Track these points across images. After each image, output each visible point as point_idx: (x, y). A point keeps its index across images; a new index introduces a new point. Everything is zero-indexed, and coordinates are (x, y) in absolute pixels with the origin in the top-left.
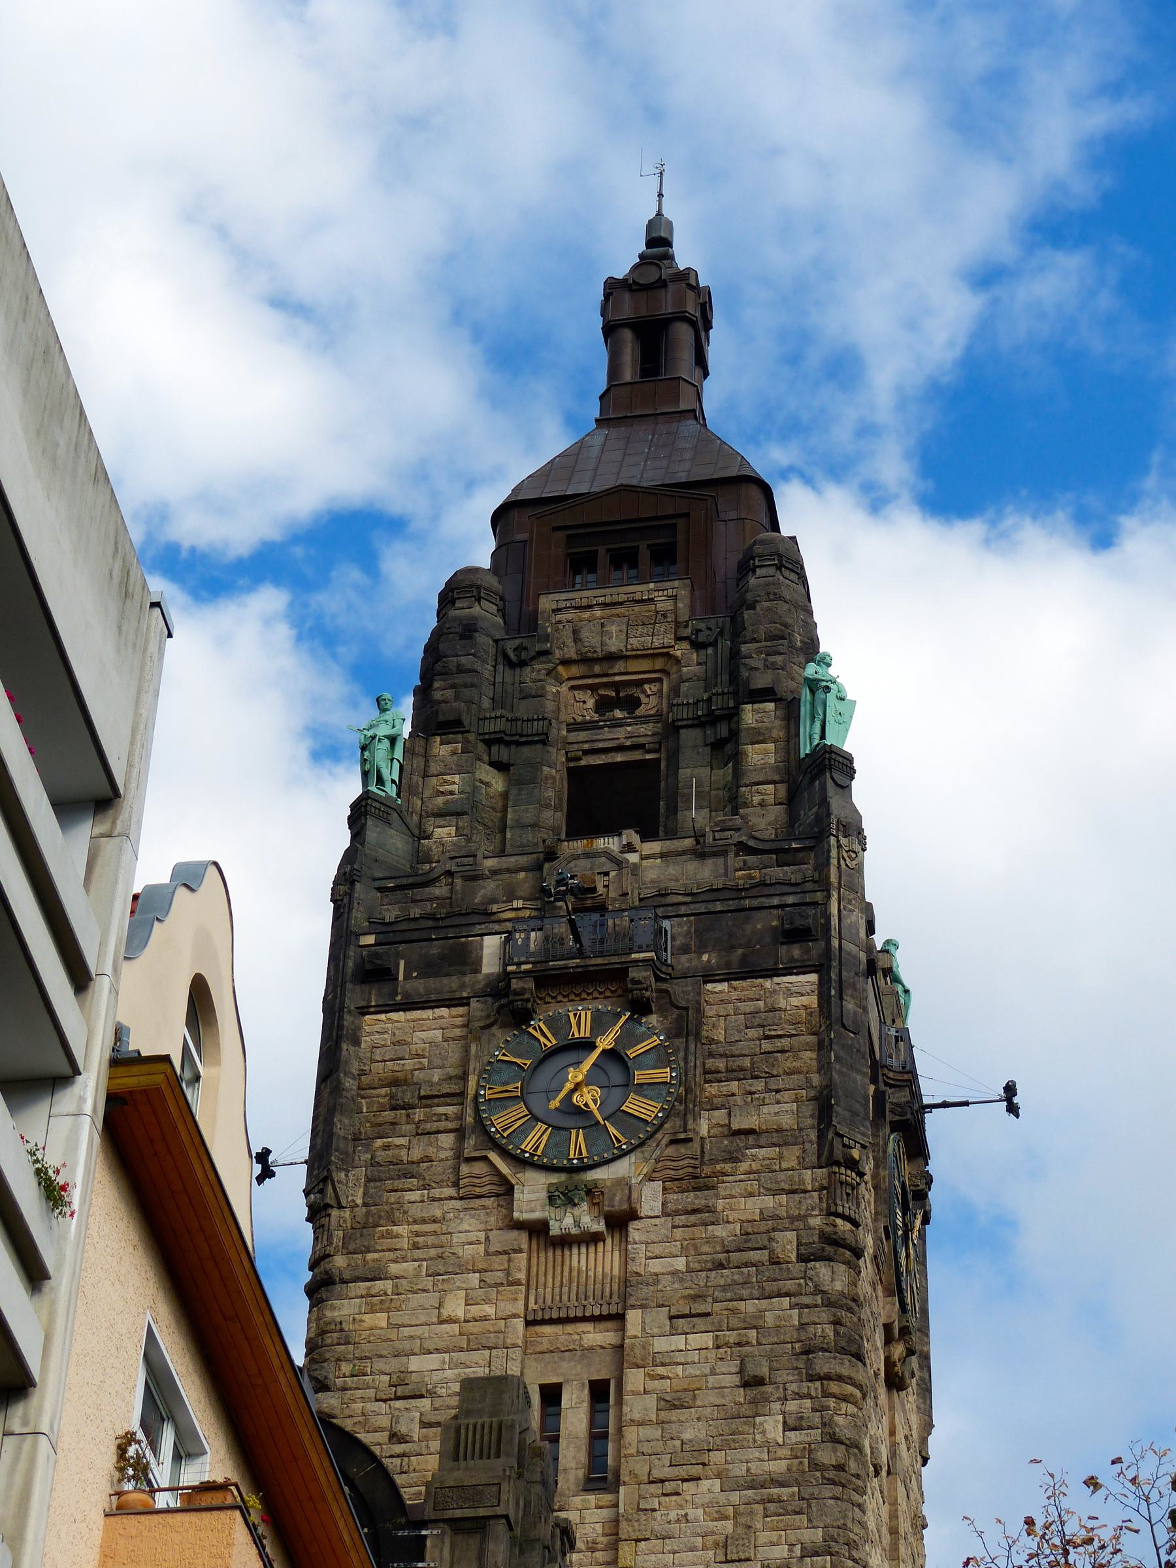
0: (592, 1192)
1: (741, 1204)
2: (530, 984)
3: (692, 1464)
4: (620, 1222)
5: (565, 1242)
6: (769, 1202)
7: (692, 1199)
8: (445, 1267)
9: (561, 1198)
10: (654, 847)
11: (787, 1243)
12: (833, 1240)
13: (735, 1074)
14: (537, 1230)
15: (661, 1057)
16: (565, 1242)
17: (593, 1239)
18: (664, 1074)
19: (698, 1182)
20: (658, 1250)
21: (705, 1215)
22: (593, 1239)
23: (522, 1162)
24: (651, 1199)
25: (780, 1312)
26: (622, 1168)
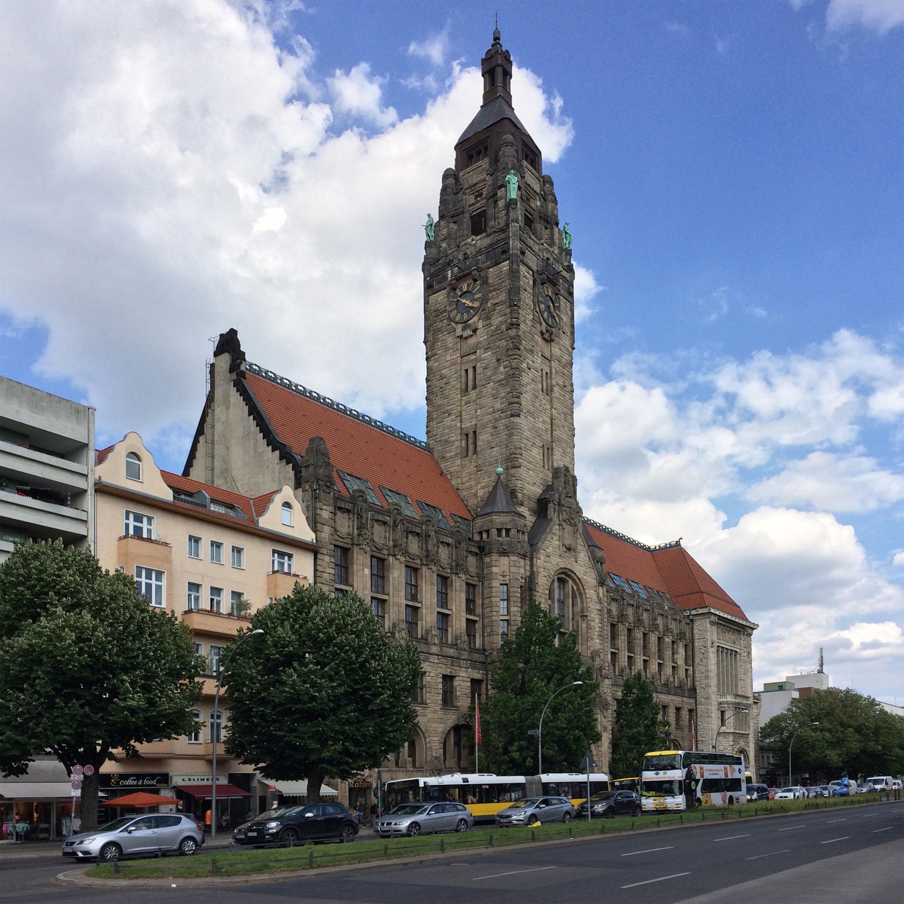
0: (469, 326)
1: (496, 320)
2: (455, 281)
3: (489, 380)
4: (475, 331)
5: (466, 338)
6: (500, 319)
7: (487, 322)
8: (447, 349)
9: (464, 329)
10: (479, 237)
11: (504, 327)
12: (512, 324)
13: (494, 290)
14: (461, 337)
15: (479, 291)
16: (466, 338)
17: (471, 336)
18: (480, 295)
19: (488, 318)
20: (482, 336)
21: (489, 325)
22: (471, 336)
23: (457, 323)
24: (480, 325)
25: (503, 343)
26: (475, 319)
